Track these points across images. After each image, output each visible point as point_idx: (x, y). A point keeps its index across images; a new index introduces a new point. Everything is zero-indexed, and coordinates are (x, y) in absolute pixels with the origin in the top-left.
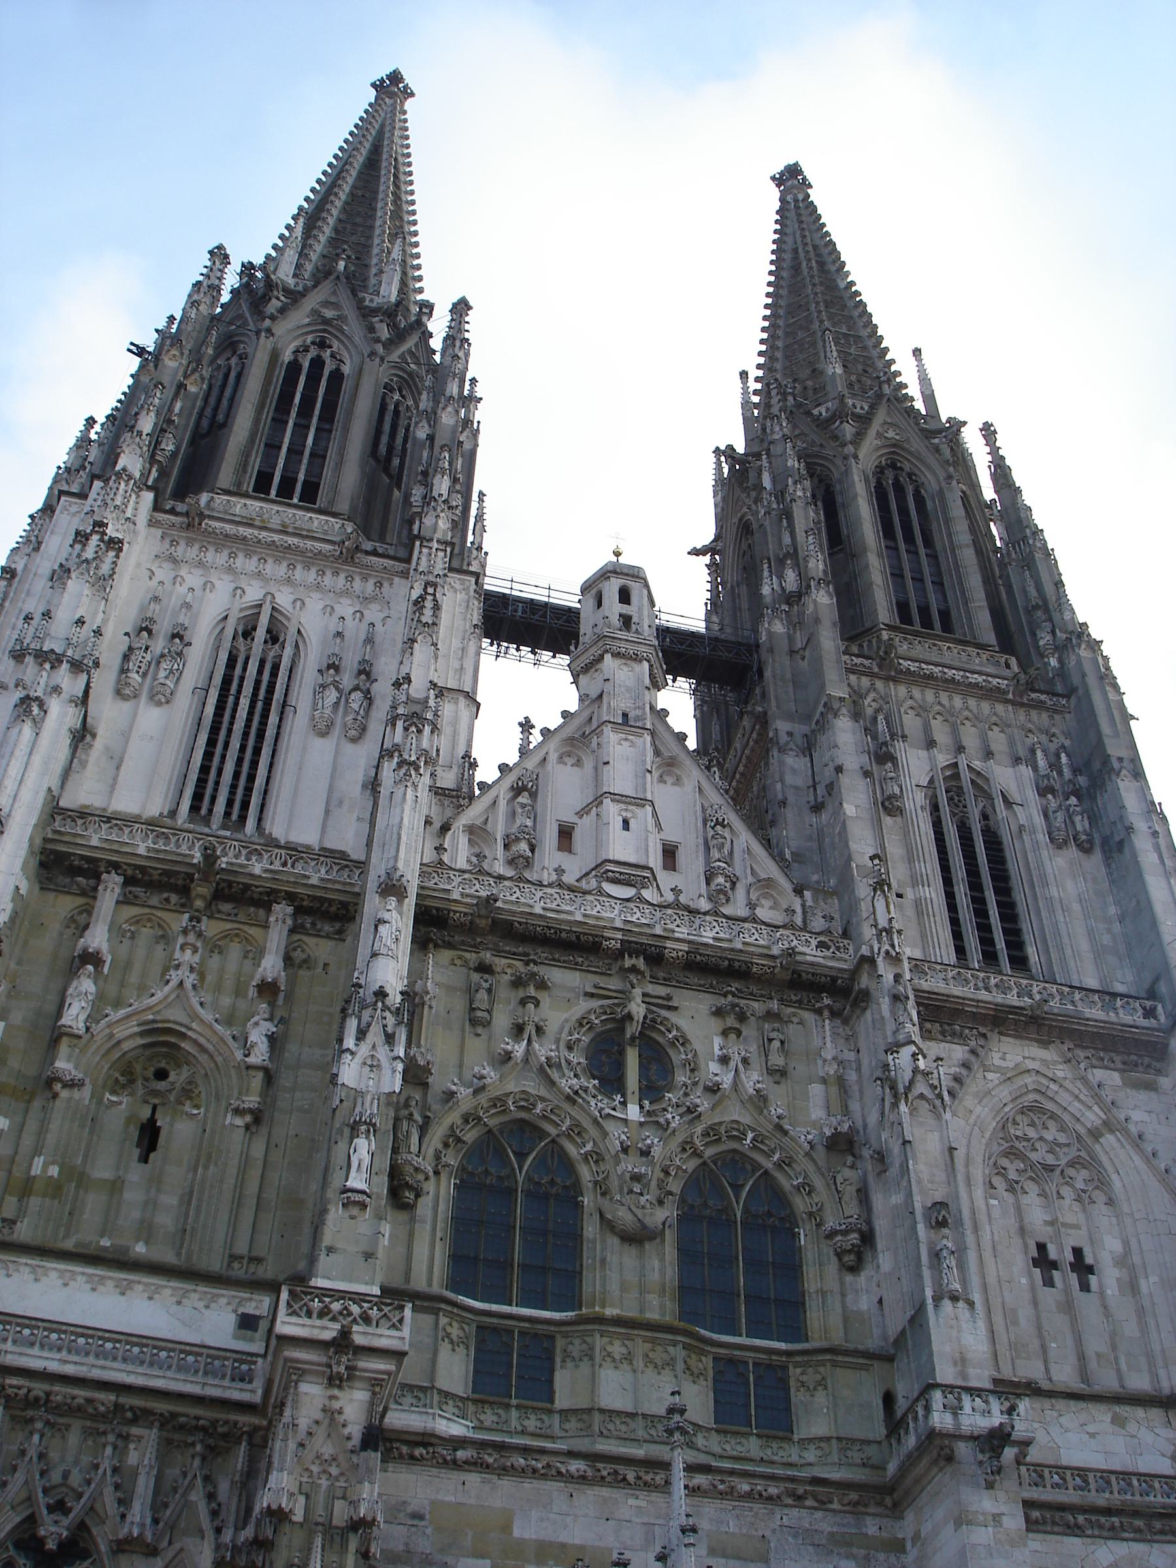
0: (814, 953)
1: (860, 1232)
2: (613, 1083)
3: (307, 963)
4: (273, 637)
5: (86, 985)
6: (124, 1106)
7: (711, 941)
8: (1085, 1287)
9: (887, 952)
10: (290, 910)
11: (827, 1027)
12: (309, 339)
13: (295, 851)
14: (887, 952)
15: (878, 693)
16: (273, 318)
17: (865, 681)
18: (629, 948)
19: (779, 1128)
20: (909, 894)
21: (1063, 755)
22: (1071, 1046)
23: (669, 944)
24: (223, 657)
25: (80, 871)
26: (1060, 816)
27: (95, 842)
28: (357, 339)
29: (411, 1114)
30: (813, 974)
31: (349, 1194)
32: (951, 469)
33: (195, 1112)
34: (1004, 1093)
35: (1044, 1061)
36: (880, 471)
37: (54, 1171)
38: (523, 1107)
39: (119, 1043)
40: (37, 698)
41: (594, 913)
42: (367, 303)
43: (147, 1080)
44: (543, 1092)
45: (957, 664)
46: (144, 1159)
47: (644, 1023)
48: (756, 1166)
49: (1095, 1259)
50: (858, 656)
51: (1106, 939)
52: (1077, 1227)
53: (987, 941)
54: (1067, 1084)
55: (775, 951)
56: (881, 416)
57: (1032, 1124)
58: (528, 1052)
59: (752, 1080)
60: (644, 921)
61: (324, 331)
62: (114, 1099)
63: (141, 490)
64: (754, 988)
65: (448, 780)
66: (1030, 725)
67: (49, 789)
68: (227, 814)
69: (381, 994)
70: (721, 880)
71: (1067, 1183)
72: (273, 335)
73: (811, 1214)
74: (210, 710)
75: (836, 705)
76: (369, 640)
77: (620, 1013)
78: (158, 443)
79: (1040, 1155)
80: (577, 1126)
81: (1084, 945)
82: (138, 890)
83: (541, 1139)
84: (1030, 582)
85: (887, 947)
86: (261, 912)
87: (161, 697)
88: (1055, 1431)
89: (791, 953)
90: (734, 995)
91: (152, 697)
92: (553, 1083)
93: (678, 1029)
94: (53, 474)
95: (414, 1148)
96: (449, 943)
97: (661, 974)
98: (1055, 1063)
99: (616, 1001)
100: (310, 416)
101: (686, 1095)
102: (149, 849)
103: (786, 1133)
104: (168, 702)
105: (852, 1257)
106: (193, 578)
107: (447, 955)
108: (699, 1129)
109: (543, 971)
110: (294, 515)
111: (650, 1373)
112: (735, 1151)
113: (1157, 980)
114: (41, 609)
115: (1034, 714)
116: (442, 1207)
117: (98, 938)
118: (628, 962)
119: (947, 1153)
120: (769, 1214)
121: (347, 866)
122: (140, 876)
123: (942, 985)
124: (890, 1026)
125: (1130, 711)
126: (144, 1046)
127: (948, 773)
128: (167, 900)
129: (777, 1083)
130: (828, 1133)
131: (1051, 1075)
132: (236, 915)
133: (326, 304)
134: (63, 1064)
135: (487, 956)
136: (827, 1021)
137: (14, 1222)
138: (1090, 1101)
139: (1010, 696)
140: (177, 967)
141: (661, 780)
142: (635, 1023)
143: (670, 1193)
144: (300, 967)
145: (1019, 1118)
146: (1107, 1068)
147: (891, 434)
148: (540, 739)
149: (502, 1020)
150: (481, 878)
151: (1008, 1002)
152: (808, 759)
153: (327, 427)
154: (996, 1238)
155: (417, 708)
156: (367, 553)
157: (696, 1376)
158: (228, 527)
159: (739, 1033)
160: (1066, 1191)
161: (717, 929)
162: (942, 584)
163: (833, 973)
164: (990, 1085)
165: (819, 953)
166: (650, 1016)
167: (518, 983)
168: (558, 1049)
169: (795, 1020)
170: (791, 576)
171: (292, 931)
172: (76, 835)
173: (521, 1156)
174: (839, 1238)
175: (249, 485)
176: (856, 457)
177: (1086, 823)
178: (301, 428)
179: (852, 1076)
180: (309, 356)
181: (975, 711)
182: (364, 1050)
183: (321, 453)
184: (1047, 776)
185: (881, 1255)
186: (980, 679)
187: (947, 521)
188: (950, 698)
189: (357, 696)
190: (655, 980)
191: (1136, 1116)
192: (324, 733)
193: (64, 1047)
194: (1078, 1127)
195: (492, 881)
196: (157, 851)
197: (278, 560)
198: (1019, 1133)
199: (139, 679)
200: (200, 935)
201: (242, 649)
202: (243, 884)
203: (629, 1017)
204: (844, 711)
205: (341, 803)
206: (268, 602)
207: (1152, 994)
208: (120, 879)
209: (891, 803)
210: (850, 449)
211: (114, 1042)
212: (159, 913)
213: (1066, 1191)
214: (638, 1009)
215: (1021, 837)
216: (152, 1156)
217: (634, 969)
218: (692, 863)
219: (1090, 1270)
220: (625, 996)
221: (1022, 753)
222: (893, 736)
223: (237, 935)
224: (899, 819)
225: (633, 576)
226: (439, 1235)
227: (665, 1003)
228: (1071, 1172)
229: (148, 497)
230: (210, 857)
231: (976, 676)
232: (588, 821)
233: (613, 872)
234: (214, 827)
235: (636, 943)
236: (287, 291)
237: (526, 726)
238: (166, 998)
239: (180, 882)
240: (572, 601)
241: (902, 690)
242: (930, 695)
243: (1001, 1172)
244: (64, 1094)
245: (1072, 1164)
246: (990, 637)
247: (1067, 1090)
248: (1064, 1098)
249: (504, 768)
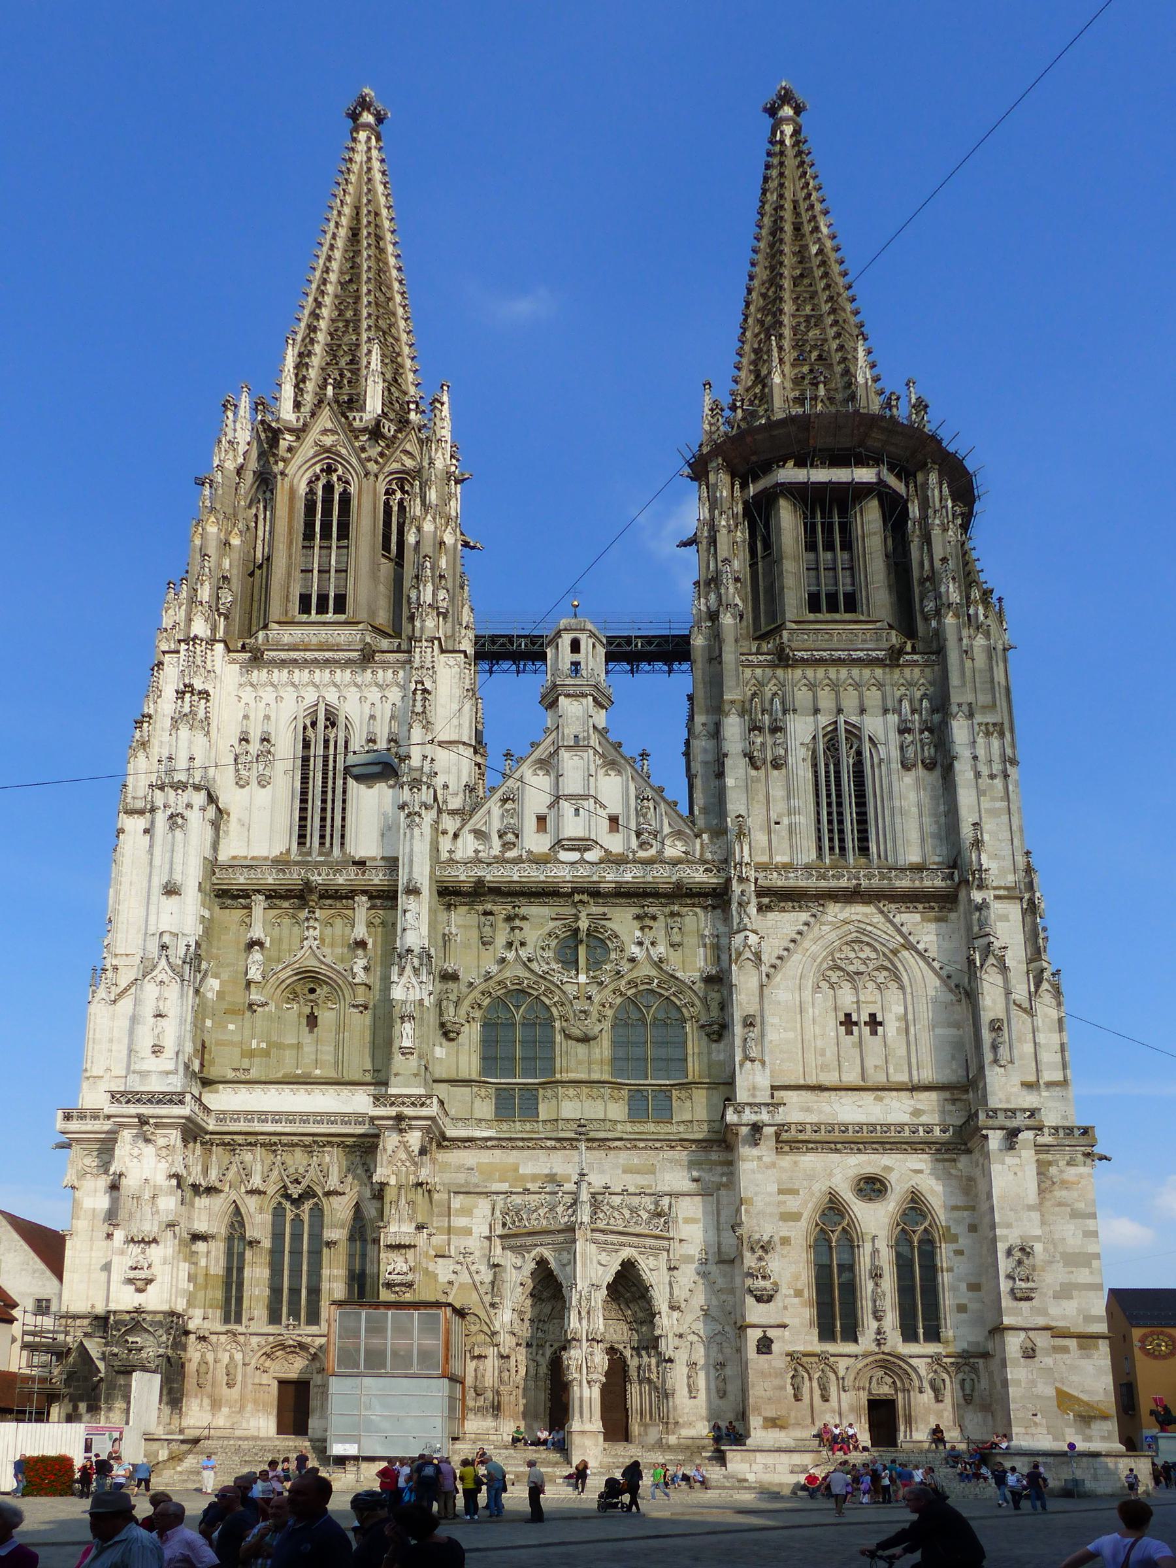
5: (257, 955)
52: (875, 1002)
59: (661, 949)
88: (836, 1106)
111: (590, 1101)
134: (254, 997)
149: (501, 939)
157: (616, 1100)
173: (518, 1007)
213: (871, 985)
219: (880, 1024)
228: (876, 973)
243: (826, 979)
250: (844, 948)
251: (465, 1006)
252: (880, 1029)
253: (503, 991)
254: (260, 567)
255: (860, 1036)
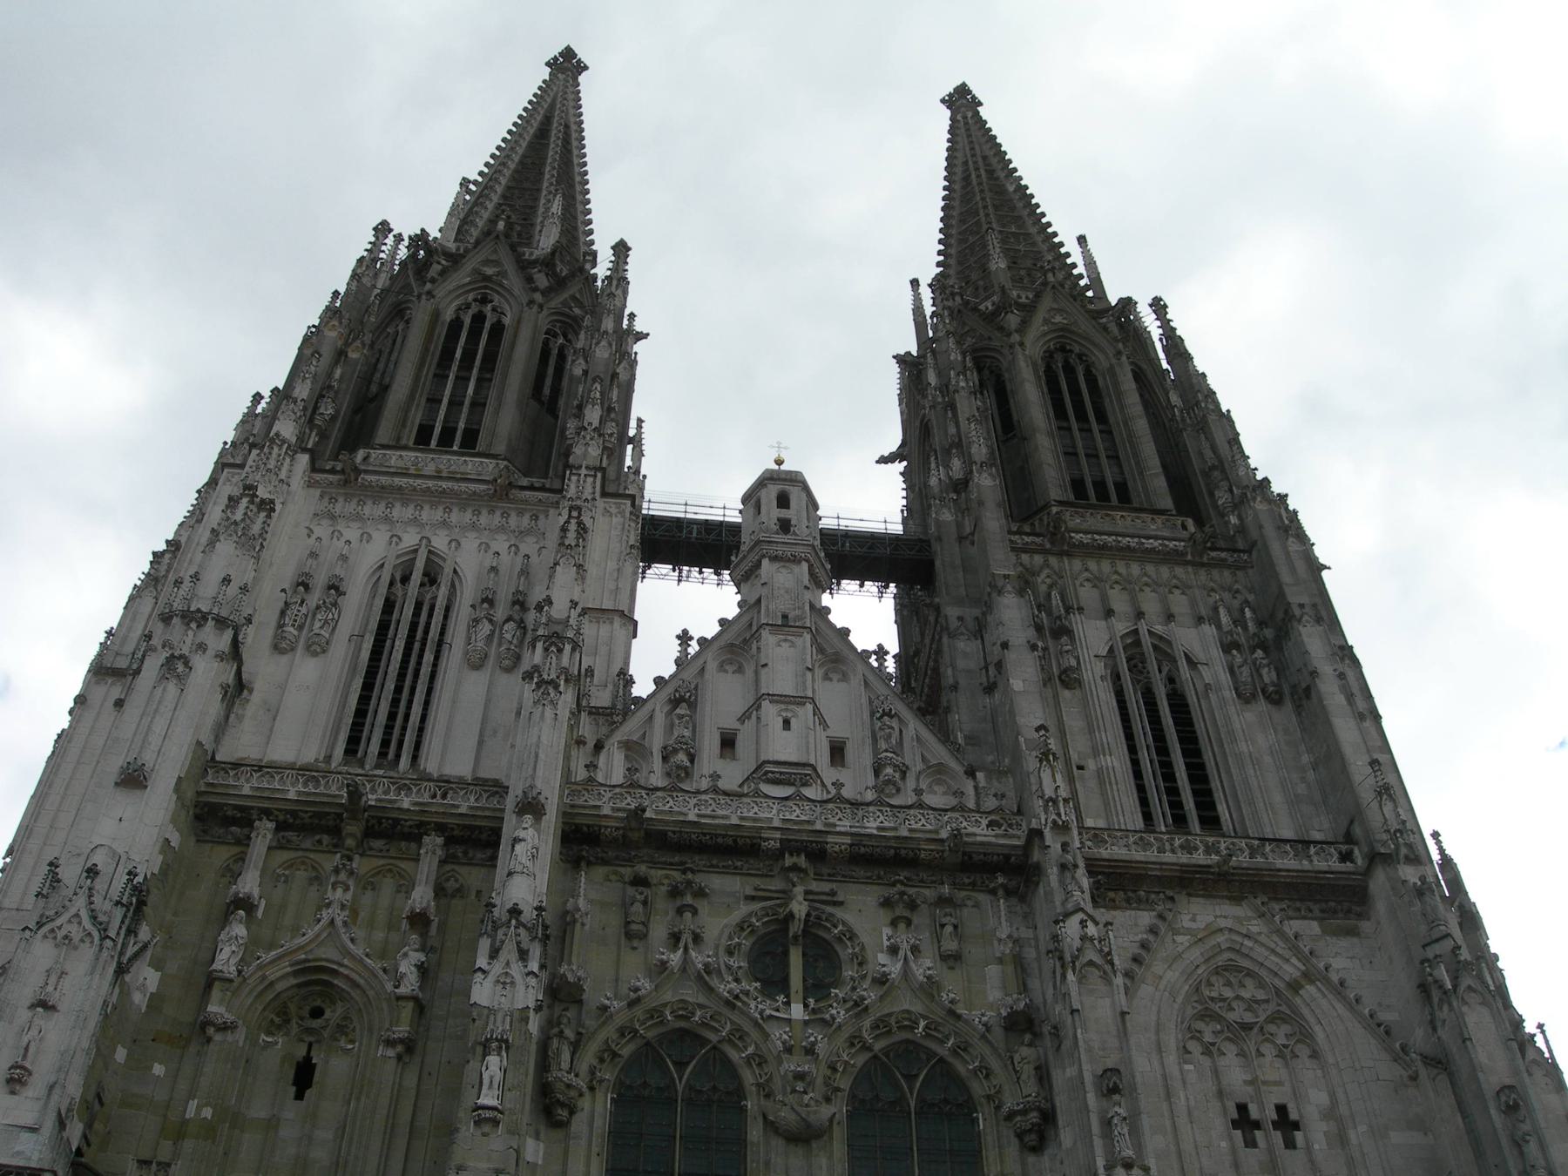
0: (985, 832)
1: (1039, 1109)
2: (776, 984)
3: (460, 892)
4: (431, 578)
5: (239, 930)
6: (279, 1046)
7: (875, 832)
8: (1290, 1144)
9: (1054, 822)
10: (440, 841)
11: (1002, 908)
12: (471, 297)
13: (446, 784)
14: (1054, 822)
15: (1052, 568)
16: (433, 281)
17: (1038, 559)
18: (788, 846)
19: (952, 1013)
20: (1091, 765)
21: (1247, 609)
22: (1266, 900)
23: (830, 839)
24: (379, 603)
25: (234, 821)
26: (1245, 671)
27: (246, 791)
28: (516, 291)
29: (562, 1032)
30: (985, 854)
31: (480, 1112)
32: (1120, 345)
33: (350, 1047)
34: (1195, 955)
35: (1238, 919)
36: (1049, 356)
37: (207, 1113)
38: (682, 1016)
39: (272, 984)
40: (182, 657)
41: (751, 814)
42: (527, 257)
43: (302, 1019)
44: (701, 1000)
45: (1131, 531)
46: (299, 1096)
47: (806, 921)
48: (933, 1054)
49: (1301, 1116)
50: (1028, 534)
51: (1301, 789)
52: (1279, 1083)
53: (1176, 805)
54: (1263, 939)
55: (944, 834)
56: (1047, 302)
57: (1229, 984)
58: (686, 961)
60: (803, 818)
61: (486, 287)
62: (270, 1040)
63: (296, 452)
64: (924, 875)
65: (601, 698)
66: (1212, 584)
67: (199, 743)
68: (383, 754)
69: (515, 912)
70: (889, 770)
71: (1267, 1040)
72: (433, 297)
73: (989, 1097)
74: (365, 655)
75: (1000, 583)
76: (525, 572)
77: (782, 912)
78: (316, 408)
79: (1238, 1014)
80: (738, 1030)
81: (1278, 798)
82: (289, 834)
83: (702, 1046)
84: (1206, 445)
85: (1054, 817)
86: (413, 845)
87: (317, 648)
89: (957, 835)
90: (902, 883)
91: (308, 648)
92: (711, 989)
93: (844, 923)
94: (219, 450)
95: (565, 1065)
96: (602, 859)
97: (825, 871)
98: (1249, 919)
99: (778, 902)
100: (470, 368)
101: (854, 989)
102: (299, 793)
103: (959, 1017)
104: (324, 652)
105: (1033, 1136)
106: (352, 532)
107: (600, 872)
108: (867, 1023)
109: (700, 879)
110: (449, 460)
112: (908, 1041)
113: (1352, 822)
114: (192, 572)
115: (1215, 573)
116: (598, 1122)
117: (249, 884)
118: (789, 861)
119: (1119, 1019)
120: (946, 1101)
121: (497, 793)
122: (291, 821)
123: (1124, 851)
124: (1058, 898)
125: (1322, 561)
126: (299, 986)
127: (1129, 641)
128: (320, 842)
129: (951, 968)
130: (1004, 1014)
131: (1244, 932)
132: (388, 850)
133: (487, 262)
134: (216, 1008)
135: (642, 869)
136: (1002, 901)
137: (169, 1165)
138: (1287, 954)
139: (1189, 557)
140: (328, 905)
141: (827, 678)
142: (796, 921)
143: (838, 1090)
144: (453, 896)
145: (1213, 979)
146: (1304, 918)
147: (1058, 319)
148: (697, 648)
149: (659, 931)
150: (632, 791)
151: (1193, 862)
152: (979, 641)
153: (488, 376)
154: (1192, 1103)
155: (558, 628)
156: (523, 488)
158: (384, 480)
159: (909, 923)
160: (1268, 1049)
161: (882, 818)
162: (1117, 457)
163: (1006, 851)
164: (1180, 949)
165: (990, 832)
166: (814, 914)
167: (675, 893)
168: (716, 955)
169: (969, 903)
170: (956, 463)
171: (442, 862)
172: (227, 786)
173: (681, 1066)
174: (1019, 1118)
175: (410, 437)
176: (1021, 344)
177: (1274, 674)
178: (462, 380)
179: (1030, 954)
180: (470, 312)
181: (1154, 577)
182: (497, 968)
183: (482, 401)
184: (1230, 632)
185: (1062, 1131)
186: (1156, 543)
187: (1119, 394)
188: (1128, 566)
189: (510, 626)
190: (819, 877)
191: (1338, 963)
192: (477, 666)
193: (216, 993)
194: (1277, 982)
195: (643, 793)
196: (308, 794)
197: (434, 506)
198: (1214, 994)
199: (296, 633)
200: (351, 873)
201: (400, 594)
202: (393, 819)
203: (791, 916)
204: (1009, 588)
205: (495, 732)
206: (423, 546)
207: (1349, 838)
208: (272, 825)
209: (1068, 676)
210: (1016, 338)
211: (266, 983)
212: (312, 856)
213: (1268, 1049)
214: (799, 908)
215: (1207, 697)
216: (308, 1092)
217: (795, 868)
218: (860, 757)
219: (1296, 1126)
220: (787, 896)
221: (1203, 613)
222: (1068, 609)
223: (390, 871)
224: (1077, 692)
225: (791, 481)
226: (595, 1150)
227: (829, 898)
228: (1272, 1028)
229: (304, 459)
230: (355, 794)
231: (1151, 541)
232: (750, 725)
233: (773, 772)
234: (367, 767)
235: (797, 841)
236: (447, 255)
237: (684, 638)
238: (318, 936)
239: (331, 823)
240: (734, 517)
241: (1077, 564)
242: (1106, 566)
243: (1196, 1036)
244: (218, 1037)
245: (1271, 1020)
246: (1167, 502)
247: (1263, 945)
248: (1260, 953)
249: (659, 681)
250: (1218, 982)
251: (588, 1057)
252: (1299, 1135)
253: (662, 1030)
254: (372, 400)
255: (1271, 1150)
